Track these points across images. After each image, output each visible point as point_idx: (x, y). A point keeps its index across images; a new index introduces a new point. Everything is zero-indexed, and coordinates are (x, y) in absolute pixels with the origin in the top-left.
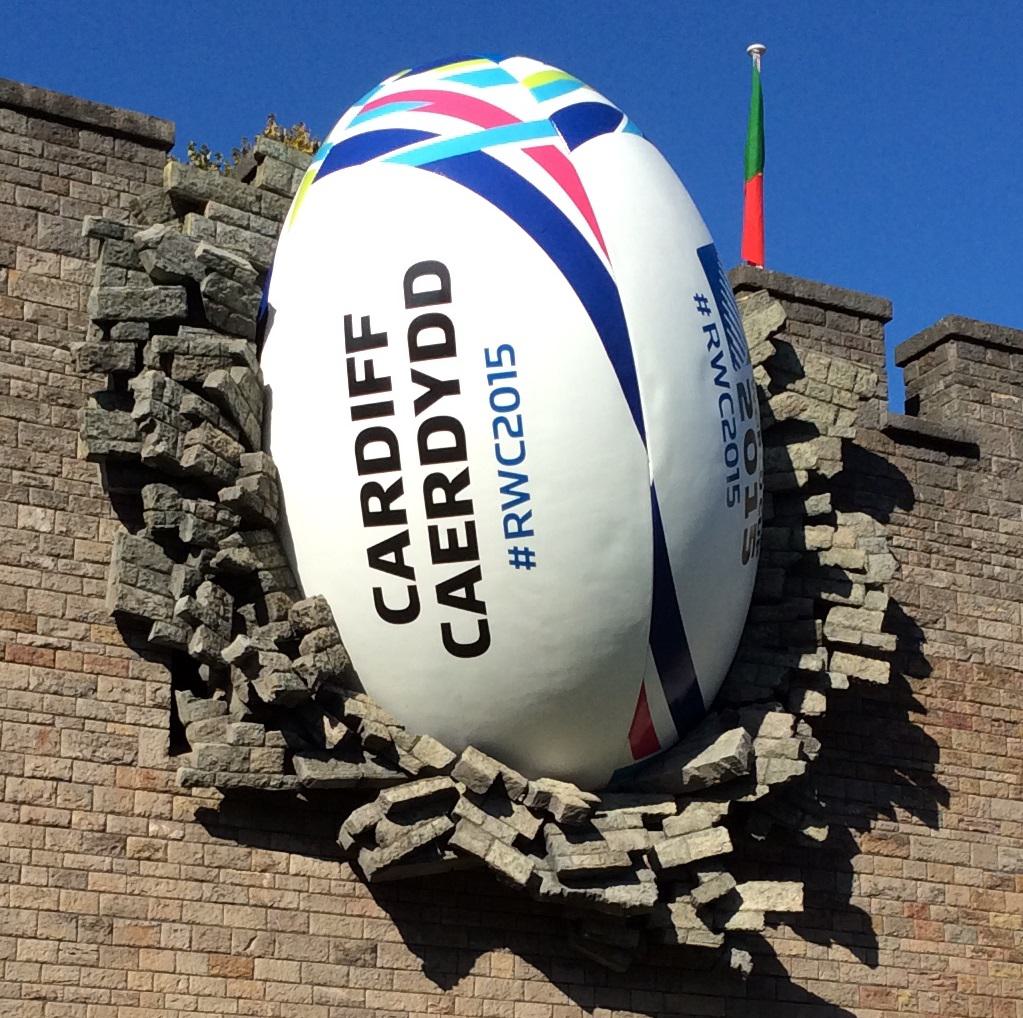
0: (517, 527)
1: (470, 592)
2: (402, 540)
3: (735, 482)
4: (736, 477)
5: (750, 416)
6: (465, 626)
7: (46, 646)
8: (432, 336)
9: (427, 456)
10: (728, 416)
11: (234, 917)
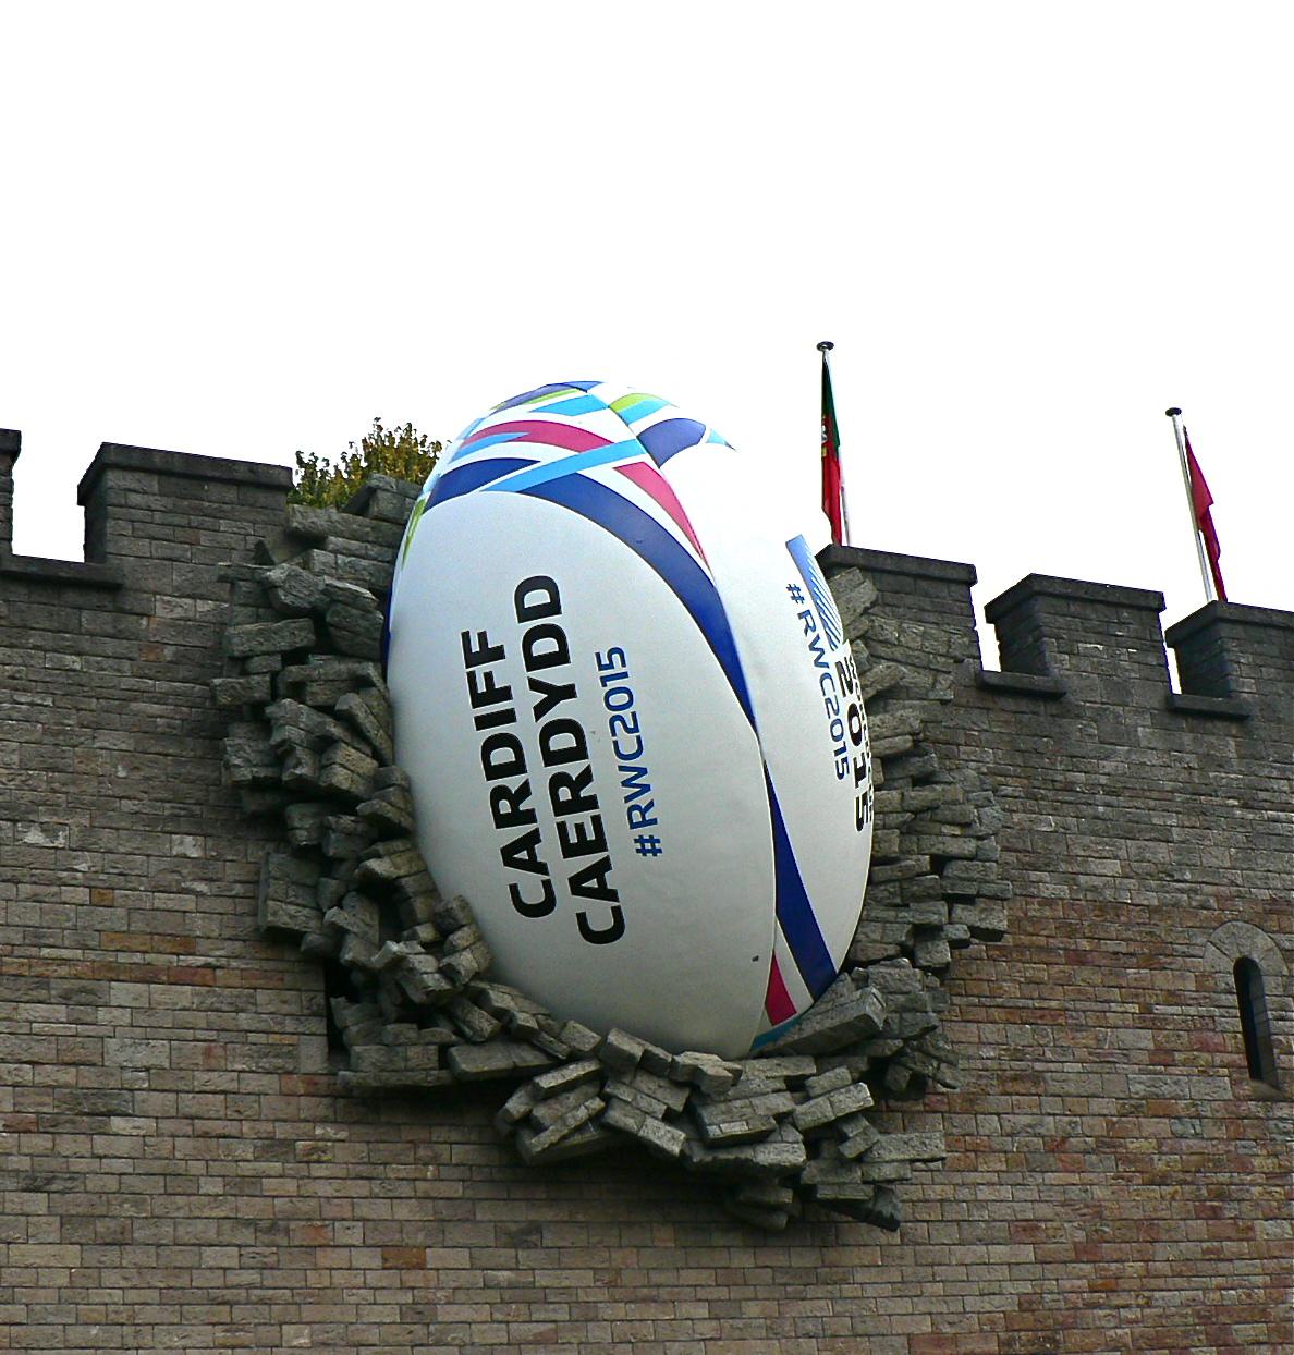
0: (641, 817)
1: (602, 882)
2: (534, 837)
3: (843, 756)
4: (843, 750)
5: (851, 691)
6: (600, 917)
7: (207, 966)
8: (545, 646)
9: (550, 758)
10: (830, 694)
11: (403, 1211)
